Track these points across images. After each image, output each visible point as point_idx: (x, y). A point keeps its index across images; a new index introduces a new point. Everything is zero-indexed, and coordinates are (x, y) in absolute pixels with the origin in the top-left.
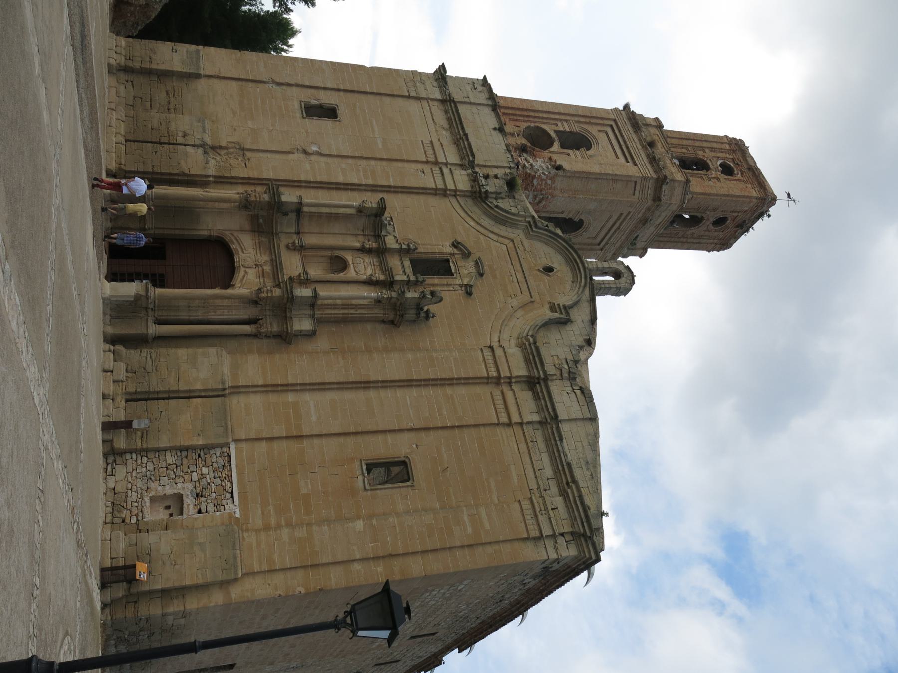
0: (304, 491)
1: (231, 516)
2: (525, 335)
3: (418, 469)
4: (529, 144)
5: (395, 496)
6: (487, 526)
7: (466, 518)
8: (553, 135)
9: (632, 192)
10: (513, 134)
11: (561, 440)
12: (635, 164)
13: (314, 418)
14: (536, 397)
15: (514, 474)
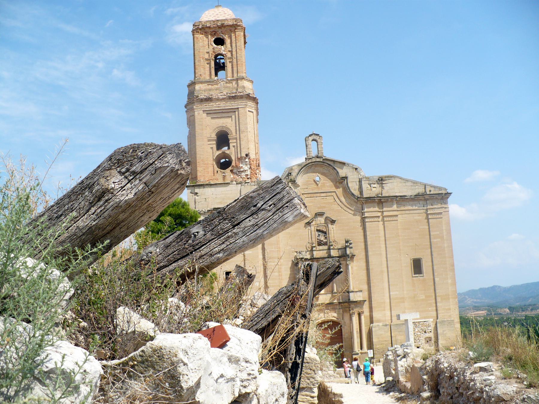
0: (424, 297)
1: (432, 322)
2: (356, 200)
3: (417, 256)
4: (230, 168)
5: (426, 266)
6: (438, 233)
7: (435, 240)
8: (219, 152)
9: (252, 114)
10: (224, 177)
11: (406, 196)
12: (238, 108)
13: (398, 293)
14: (386, 202)
15: (418, 218)
